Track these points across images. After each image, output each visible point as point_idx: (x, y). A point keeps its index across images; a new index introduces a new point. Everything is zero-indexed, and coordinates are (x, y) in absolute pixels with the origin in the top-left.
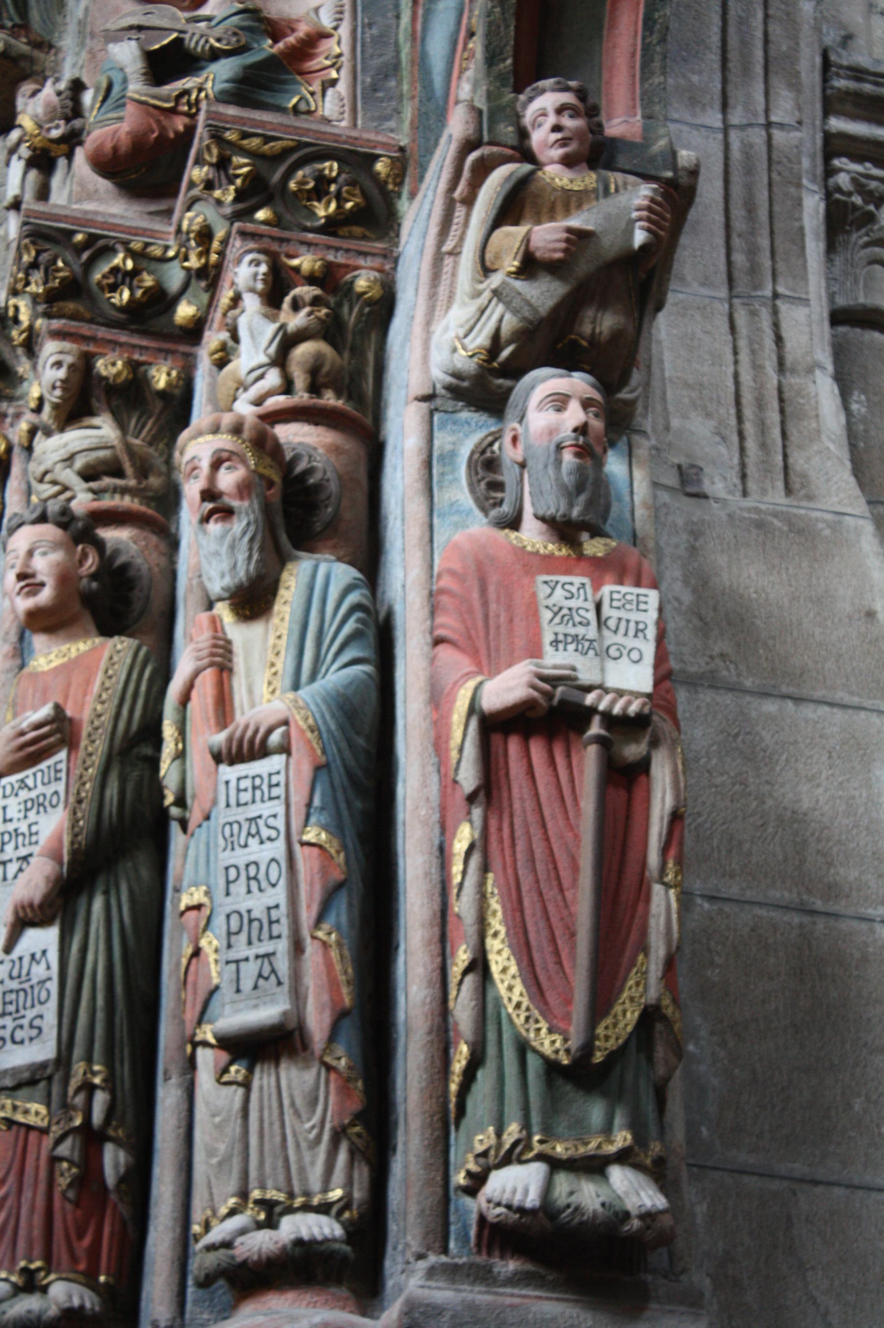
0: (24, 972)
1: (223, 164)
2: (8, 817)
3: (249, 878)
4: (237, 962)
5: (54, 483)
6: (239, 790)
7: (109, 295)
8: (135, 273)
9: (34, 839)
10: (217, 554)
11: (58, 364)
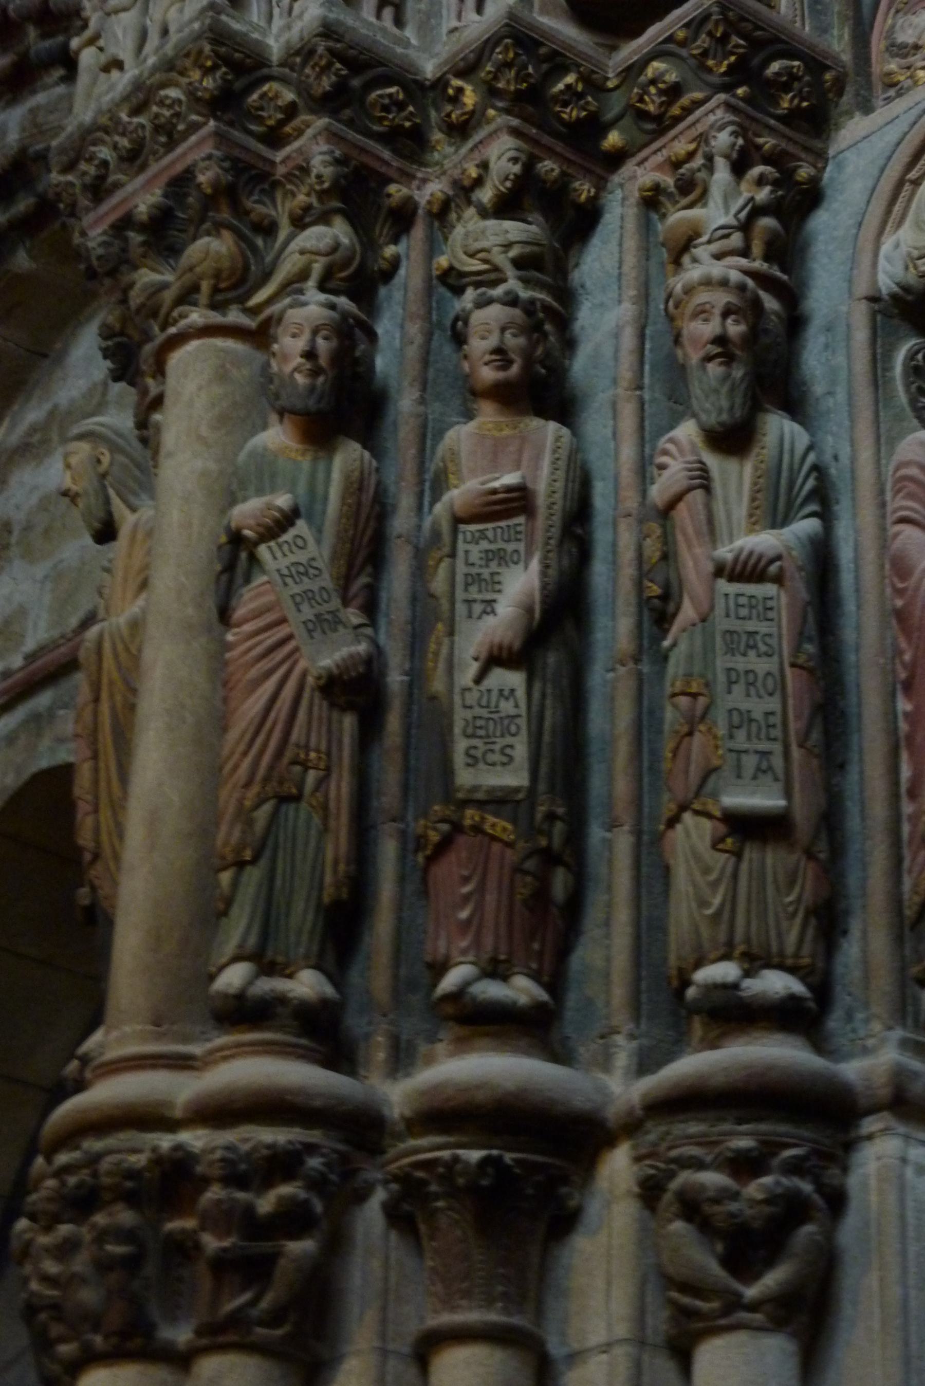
0: (493, 704)
1: (724, 40)
2: (471, 560)
3: (749, 684)
4: (739, 752)
5: (485, 261)
6: (738, 606)
7: (558, 109)
8: (580, 96)
9: (497, 587)
10: (716, 391)
11: (515, 160)
